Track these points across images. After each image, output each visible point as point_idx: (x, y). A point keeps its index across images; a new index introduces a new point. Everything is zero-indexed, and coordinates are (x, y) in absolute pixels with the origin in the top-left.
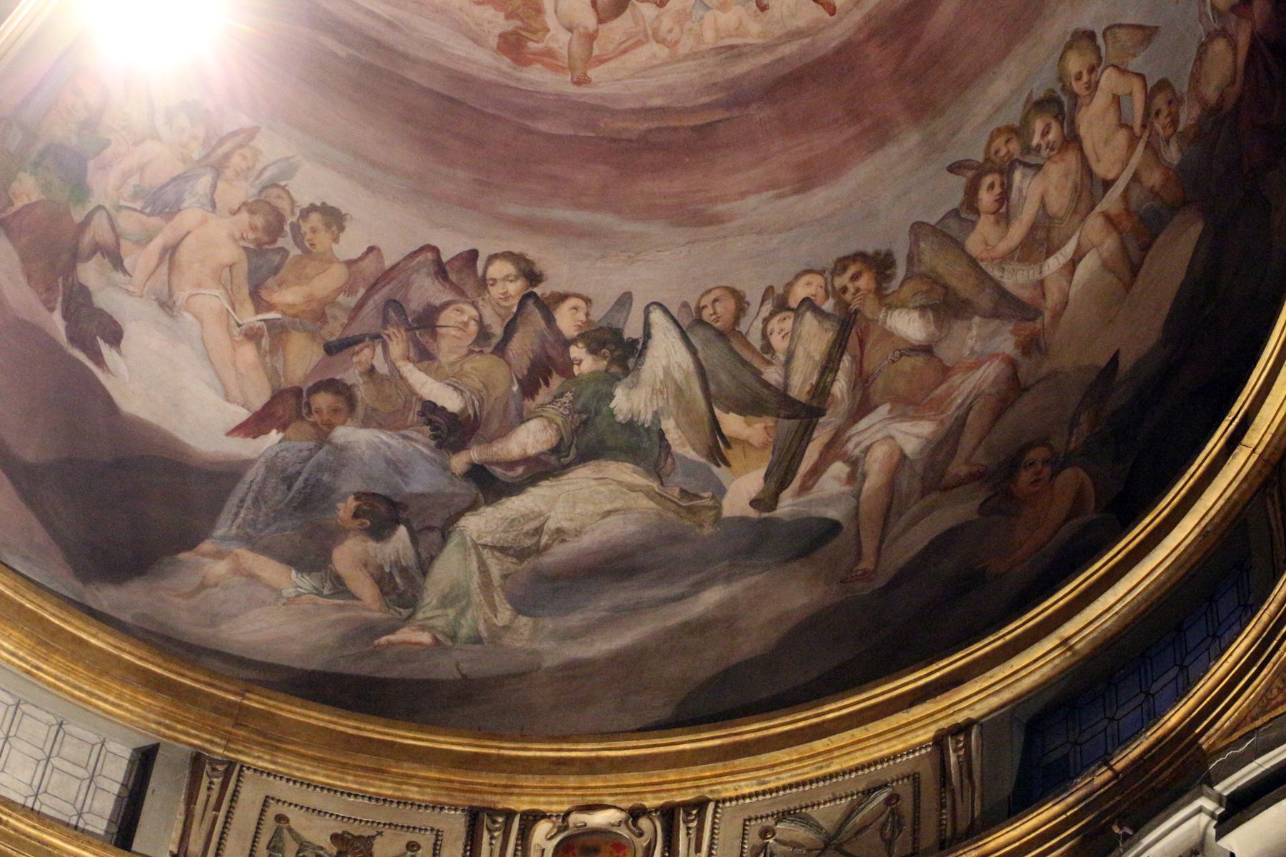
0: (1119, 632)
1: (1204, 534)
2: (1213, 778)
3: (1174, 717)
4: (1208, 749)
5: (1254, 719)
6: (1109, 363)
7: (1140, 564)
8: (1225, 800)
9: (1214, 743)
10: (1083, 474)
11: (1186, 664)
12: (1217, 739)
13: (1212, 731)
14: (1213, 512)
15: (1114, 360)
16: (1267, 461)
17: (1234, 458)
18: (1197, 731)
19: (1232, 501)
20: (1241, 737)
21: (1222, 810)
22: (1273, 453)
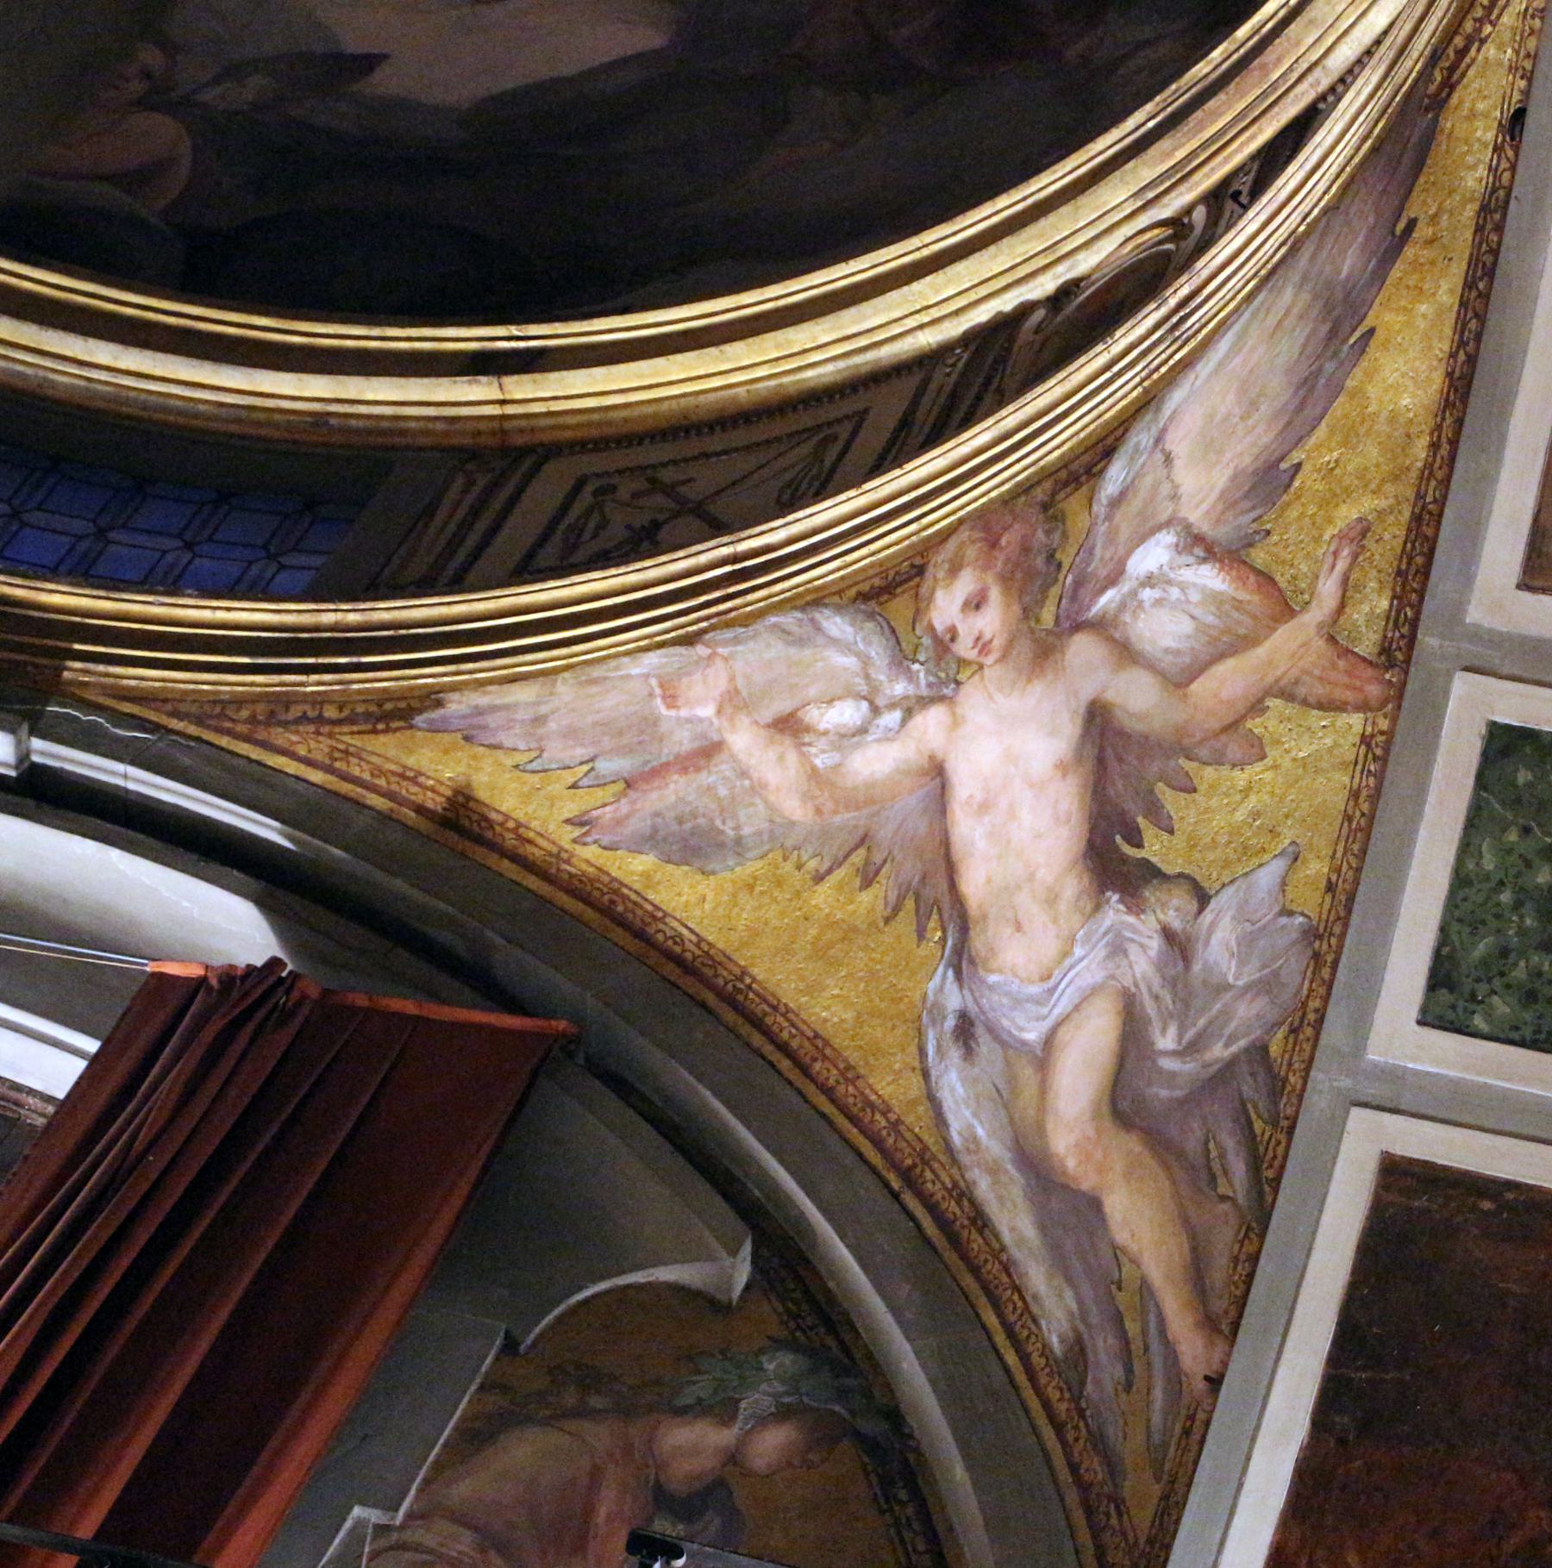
0: (58, 402)
1: (320, 419)
2: (41, 724)
3: (60, 597)
4: (71, 683)
5: (175, 714)
6: (355, 58)
7: (195, 362)
8: (26, 764)
9: (86, 684)
10: (185, 148)
11: (112, 535)
12: (94, 685)
13: (101, 668)
14: (363, 409)
15: (369, 63)
16: (504, 432)
17: (470, 382)
18: (77, 647)
19: (402, 424)
20: (133, 716)
21: (13, 773)
22: (521, 431)
